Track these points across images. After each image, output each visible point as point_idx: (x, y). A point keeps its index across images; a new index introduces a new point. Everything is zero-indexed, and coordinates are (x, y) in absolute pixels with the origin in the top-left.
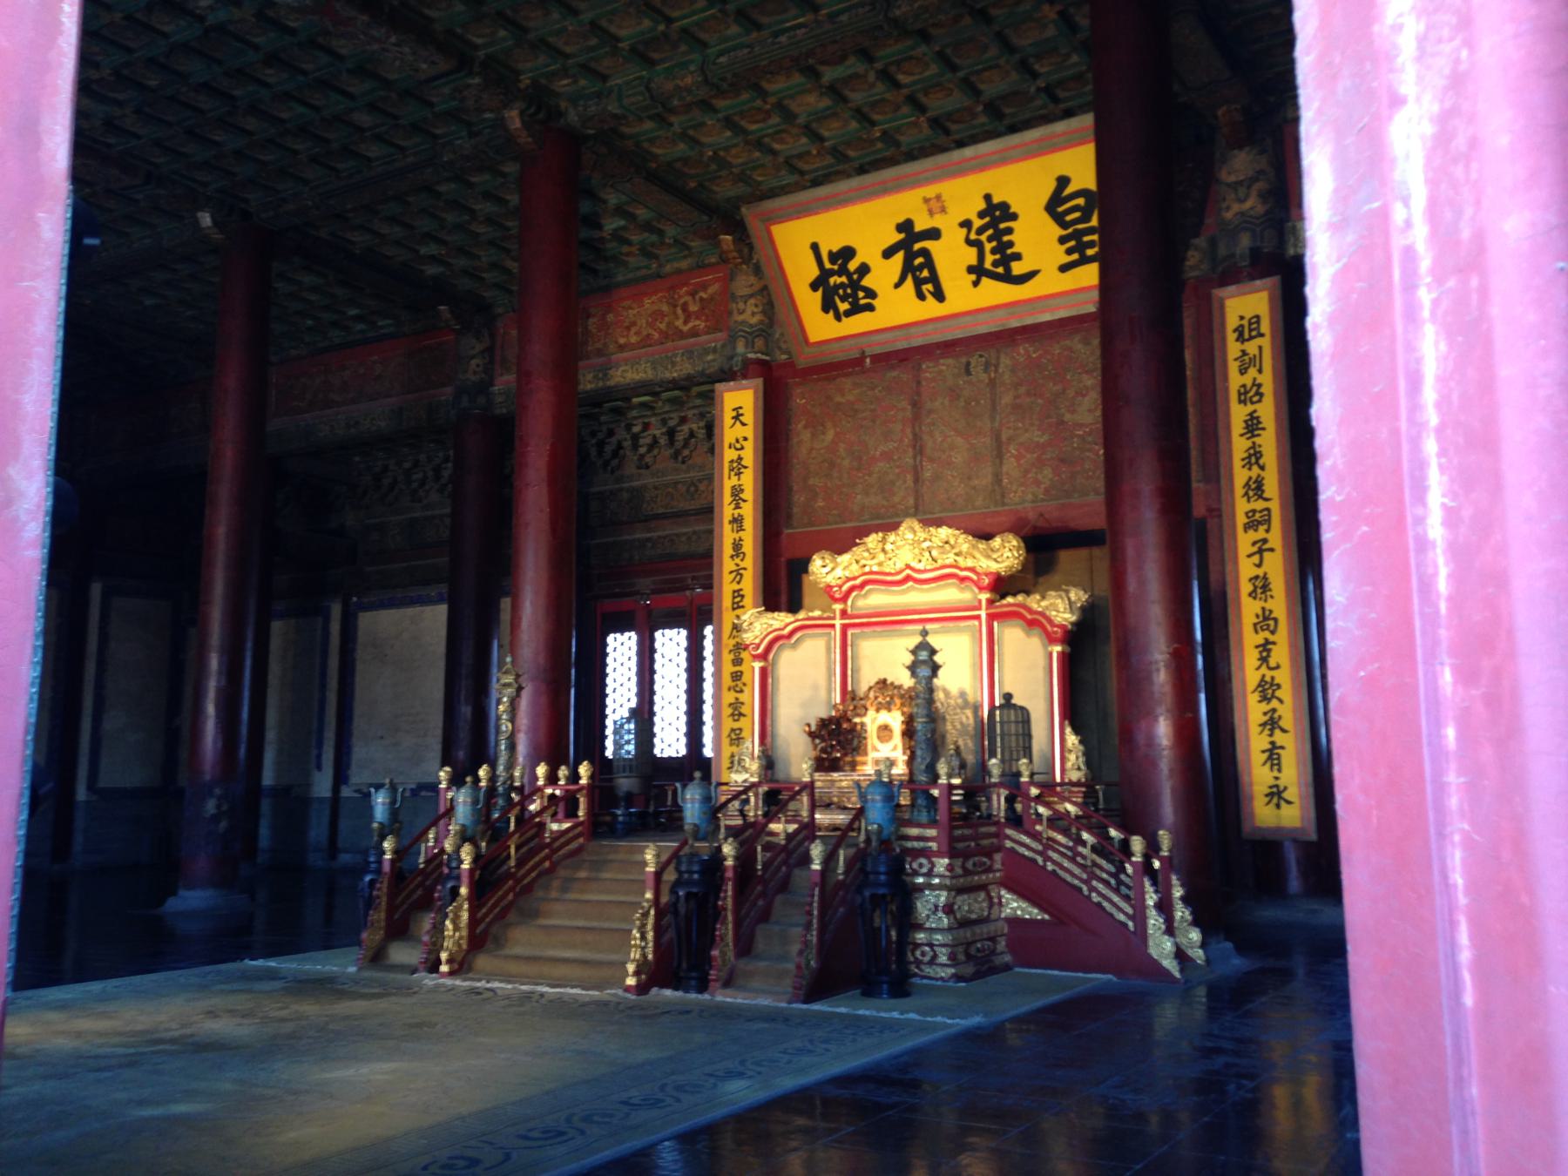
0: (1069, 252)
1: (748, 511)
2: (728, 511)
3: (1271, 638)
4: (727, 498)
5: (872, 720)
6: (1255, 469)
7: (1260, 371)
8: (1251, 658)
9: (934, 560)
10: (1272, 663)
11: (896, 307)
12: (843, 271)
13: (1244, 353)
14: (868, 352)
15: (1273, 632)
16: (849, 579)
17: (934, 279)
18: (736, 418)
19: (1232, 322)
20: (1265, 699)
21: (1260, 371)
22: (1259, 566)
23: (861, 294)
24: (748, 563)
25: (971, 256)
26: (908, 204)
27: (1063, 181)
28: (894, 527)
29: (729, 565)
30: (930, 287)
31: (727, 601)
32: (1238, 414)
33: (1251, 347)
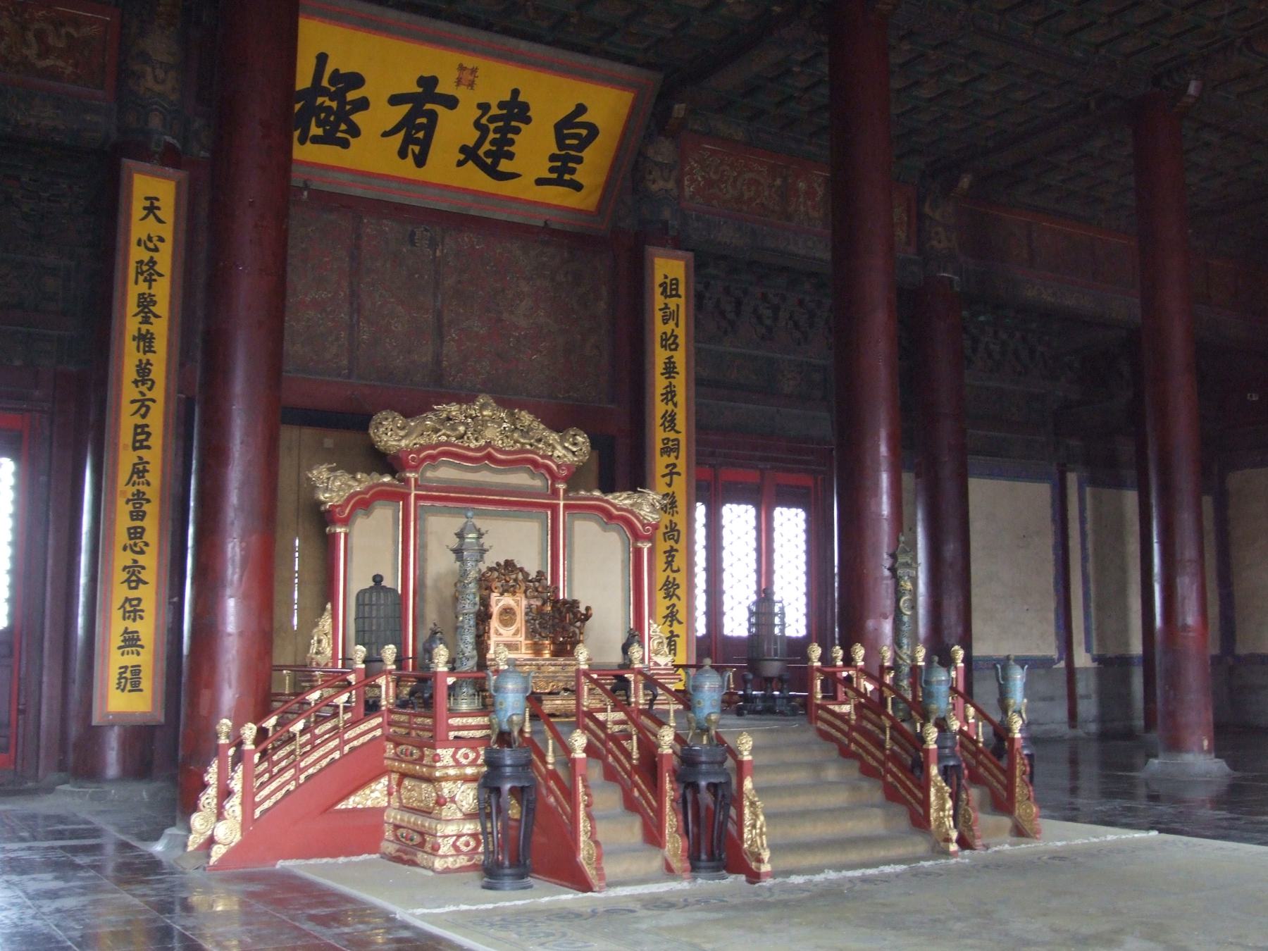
0: (552, 170)
1: (160, 329)
2: (132, 325)
3: (676, 546)
4: (132, 306)
5: (498, 602)
6: (670, 407)
7: (677, 325)
8: (661, 560)
9: (516, 442)
10: (675, 568)
11: (372, 153)
12: (339, 96)
13: (666, 307)
14: (315, 185)
15: (677, 542)
16: (424, 448)
17: (426, 144)
18: (151, 209)
19: (659, 279)
20: (669, 596)
21: (677, 325)
22: (670, 485)
23: (343, 127)
24: (158, 393)
25: (471, 137)
26: (444, 64)
27: (581, 109)
28: (469, 399)
29: (130, 392)
30: (417, 149)
31: (126, 436)
32: (660, 356)
33: (672, 303)
